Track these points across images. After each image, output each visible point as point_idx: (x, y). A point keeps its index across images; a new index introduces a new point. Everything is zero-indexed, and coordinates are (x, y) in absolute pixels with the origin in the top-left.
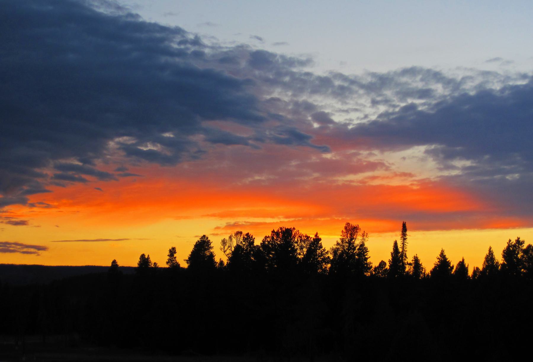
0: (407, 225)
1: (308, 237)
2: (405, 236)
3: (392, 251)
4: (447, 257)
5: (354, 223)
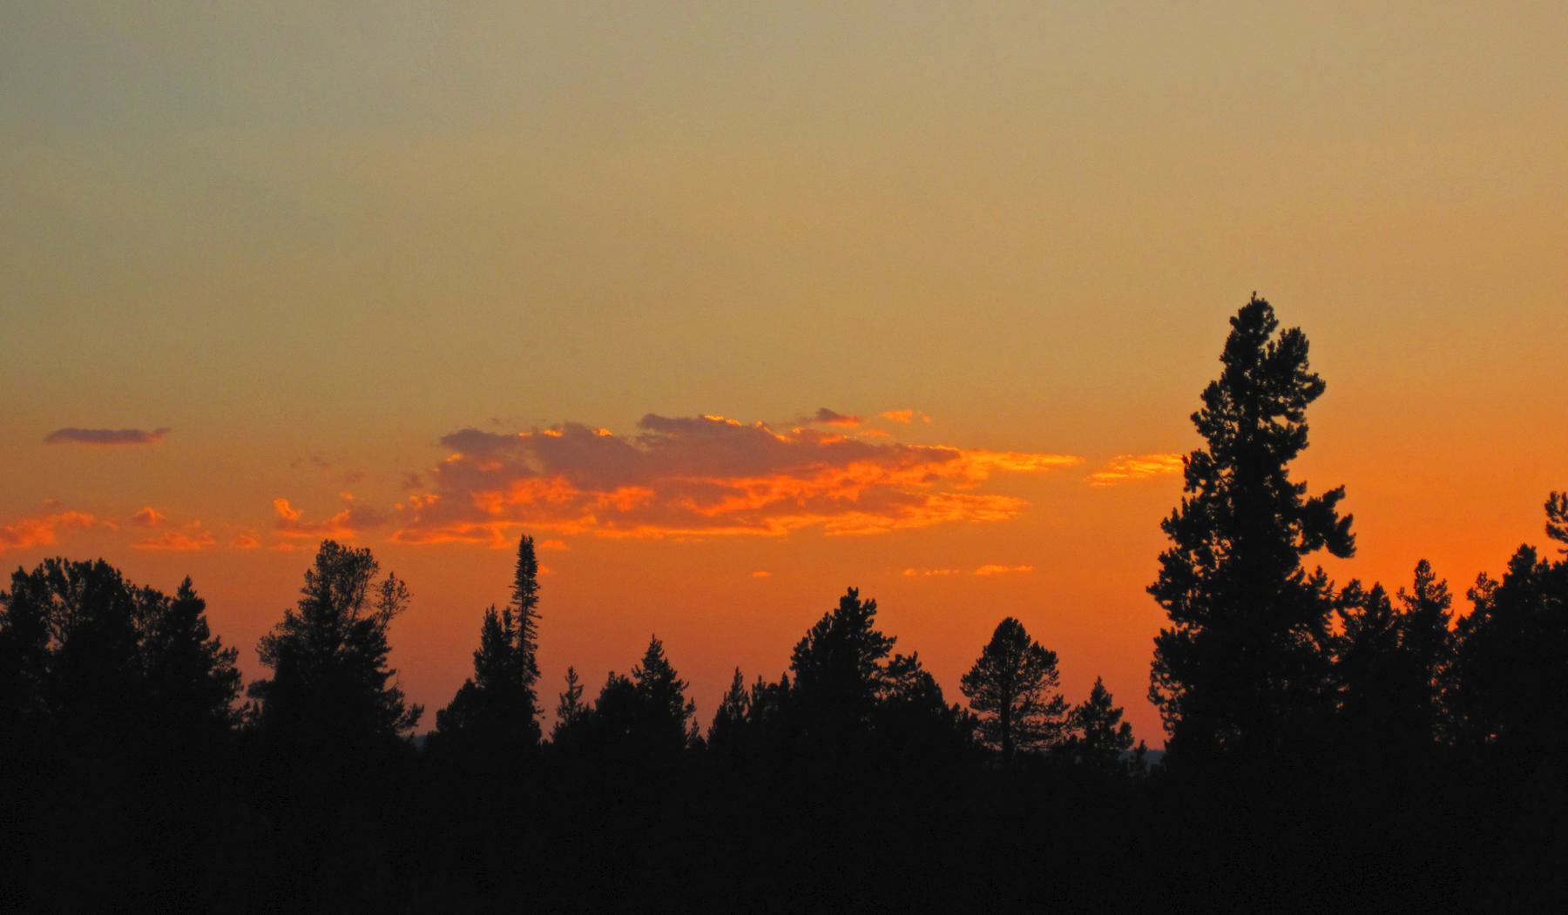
0: (539, 549)
2: (531, 591)
3: (478, 644)
4: (672, 665)
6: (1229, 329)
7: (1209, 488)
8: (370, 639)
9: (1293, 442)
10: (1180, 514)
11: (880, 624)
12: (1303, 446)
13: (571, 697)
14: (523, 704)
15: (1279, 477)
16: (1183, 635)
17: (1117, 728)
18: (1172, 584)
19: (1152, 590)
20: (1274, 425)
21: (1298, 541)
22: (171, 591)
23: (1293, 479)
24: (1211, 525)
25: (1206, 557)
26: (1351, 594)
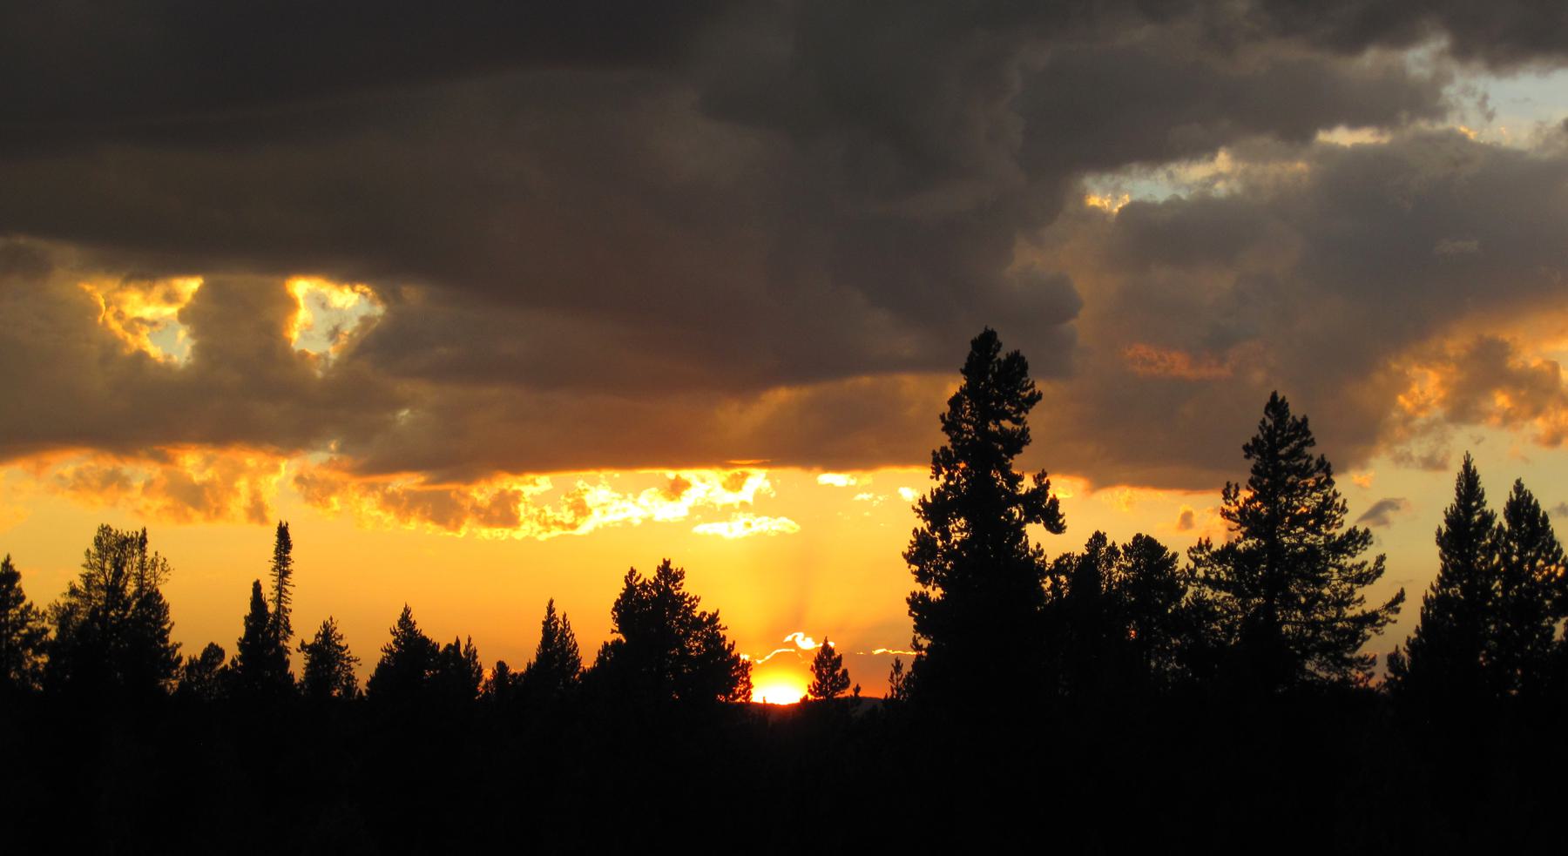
0: (291, 531)
2: (286, 565)
3: (248, 611)
6: (969, 348)
7: (950, 477)
8: (152, 604)
10: (929, 500)
11: (688, 587)
12: (1026, 443)
14: (280, 660)
17: (839, 672)
18: (921, 554)
19: (905, 556)
20: (1001, 428)
25: (946, 535)
26: (1061, 565)
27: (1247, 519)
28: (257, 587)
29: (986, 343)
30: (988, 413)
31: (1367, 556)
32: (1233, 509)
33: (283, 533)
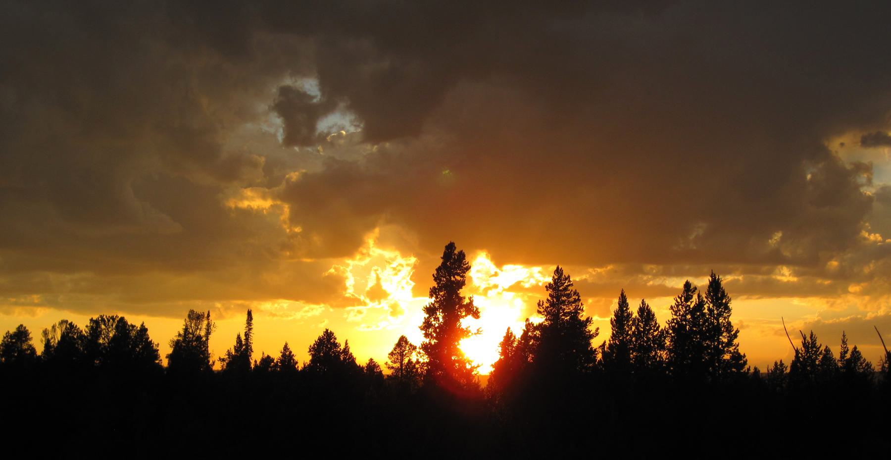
0: (254, 316)
1: (133, 326)
3: (235, 344)
5: (198, 311)
7: (437, 298)
9: (461, 284)
13: (48, 341)
15: (457, 295)
16: (430, 343)
21: (464, 314)
22: (138, 325)
23: (461, 295)
24: (437, 309)
25: (437, 319)
27: (548, 313)
28: (239, 337)
29: (450, 247)
30: (451, 274)
31: (591, 328)
32: (542, 310)
33: (249, 314)
